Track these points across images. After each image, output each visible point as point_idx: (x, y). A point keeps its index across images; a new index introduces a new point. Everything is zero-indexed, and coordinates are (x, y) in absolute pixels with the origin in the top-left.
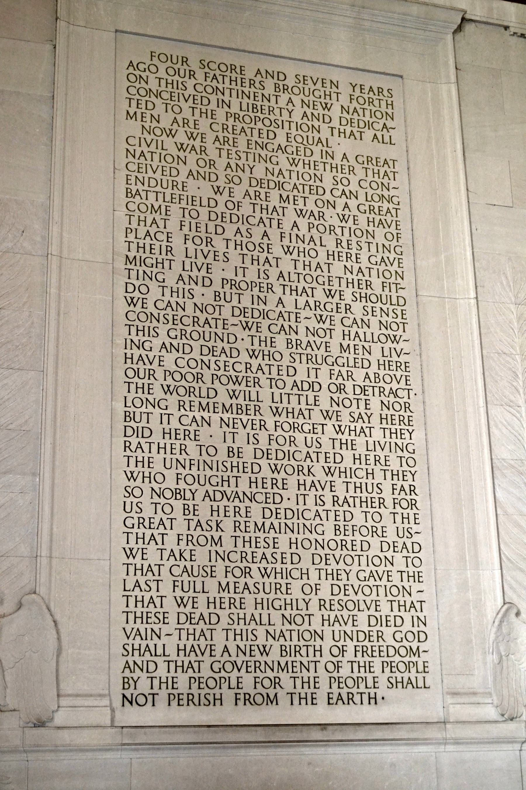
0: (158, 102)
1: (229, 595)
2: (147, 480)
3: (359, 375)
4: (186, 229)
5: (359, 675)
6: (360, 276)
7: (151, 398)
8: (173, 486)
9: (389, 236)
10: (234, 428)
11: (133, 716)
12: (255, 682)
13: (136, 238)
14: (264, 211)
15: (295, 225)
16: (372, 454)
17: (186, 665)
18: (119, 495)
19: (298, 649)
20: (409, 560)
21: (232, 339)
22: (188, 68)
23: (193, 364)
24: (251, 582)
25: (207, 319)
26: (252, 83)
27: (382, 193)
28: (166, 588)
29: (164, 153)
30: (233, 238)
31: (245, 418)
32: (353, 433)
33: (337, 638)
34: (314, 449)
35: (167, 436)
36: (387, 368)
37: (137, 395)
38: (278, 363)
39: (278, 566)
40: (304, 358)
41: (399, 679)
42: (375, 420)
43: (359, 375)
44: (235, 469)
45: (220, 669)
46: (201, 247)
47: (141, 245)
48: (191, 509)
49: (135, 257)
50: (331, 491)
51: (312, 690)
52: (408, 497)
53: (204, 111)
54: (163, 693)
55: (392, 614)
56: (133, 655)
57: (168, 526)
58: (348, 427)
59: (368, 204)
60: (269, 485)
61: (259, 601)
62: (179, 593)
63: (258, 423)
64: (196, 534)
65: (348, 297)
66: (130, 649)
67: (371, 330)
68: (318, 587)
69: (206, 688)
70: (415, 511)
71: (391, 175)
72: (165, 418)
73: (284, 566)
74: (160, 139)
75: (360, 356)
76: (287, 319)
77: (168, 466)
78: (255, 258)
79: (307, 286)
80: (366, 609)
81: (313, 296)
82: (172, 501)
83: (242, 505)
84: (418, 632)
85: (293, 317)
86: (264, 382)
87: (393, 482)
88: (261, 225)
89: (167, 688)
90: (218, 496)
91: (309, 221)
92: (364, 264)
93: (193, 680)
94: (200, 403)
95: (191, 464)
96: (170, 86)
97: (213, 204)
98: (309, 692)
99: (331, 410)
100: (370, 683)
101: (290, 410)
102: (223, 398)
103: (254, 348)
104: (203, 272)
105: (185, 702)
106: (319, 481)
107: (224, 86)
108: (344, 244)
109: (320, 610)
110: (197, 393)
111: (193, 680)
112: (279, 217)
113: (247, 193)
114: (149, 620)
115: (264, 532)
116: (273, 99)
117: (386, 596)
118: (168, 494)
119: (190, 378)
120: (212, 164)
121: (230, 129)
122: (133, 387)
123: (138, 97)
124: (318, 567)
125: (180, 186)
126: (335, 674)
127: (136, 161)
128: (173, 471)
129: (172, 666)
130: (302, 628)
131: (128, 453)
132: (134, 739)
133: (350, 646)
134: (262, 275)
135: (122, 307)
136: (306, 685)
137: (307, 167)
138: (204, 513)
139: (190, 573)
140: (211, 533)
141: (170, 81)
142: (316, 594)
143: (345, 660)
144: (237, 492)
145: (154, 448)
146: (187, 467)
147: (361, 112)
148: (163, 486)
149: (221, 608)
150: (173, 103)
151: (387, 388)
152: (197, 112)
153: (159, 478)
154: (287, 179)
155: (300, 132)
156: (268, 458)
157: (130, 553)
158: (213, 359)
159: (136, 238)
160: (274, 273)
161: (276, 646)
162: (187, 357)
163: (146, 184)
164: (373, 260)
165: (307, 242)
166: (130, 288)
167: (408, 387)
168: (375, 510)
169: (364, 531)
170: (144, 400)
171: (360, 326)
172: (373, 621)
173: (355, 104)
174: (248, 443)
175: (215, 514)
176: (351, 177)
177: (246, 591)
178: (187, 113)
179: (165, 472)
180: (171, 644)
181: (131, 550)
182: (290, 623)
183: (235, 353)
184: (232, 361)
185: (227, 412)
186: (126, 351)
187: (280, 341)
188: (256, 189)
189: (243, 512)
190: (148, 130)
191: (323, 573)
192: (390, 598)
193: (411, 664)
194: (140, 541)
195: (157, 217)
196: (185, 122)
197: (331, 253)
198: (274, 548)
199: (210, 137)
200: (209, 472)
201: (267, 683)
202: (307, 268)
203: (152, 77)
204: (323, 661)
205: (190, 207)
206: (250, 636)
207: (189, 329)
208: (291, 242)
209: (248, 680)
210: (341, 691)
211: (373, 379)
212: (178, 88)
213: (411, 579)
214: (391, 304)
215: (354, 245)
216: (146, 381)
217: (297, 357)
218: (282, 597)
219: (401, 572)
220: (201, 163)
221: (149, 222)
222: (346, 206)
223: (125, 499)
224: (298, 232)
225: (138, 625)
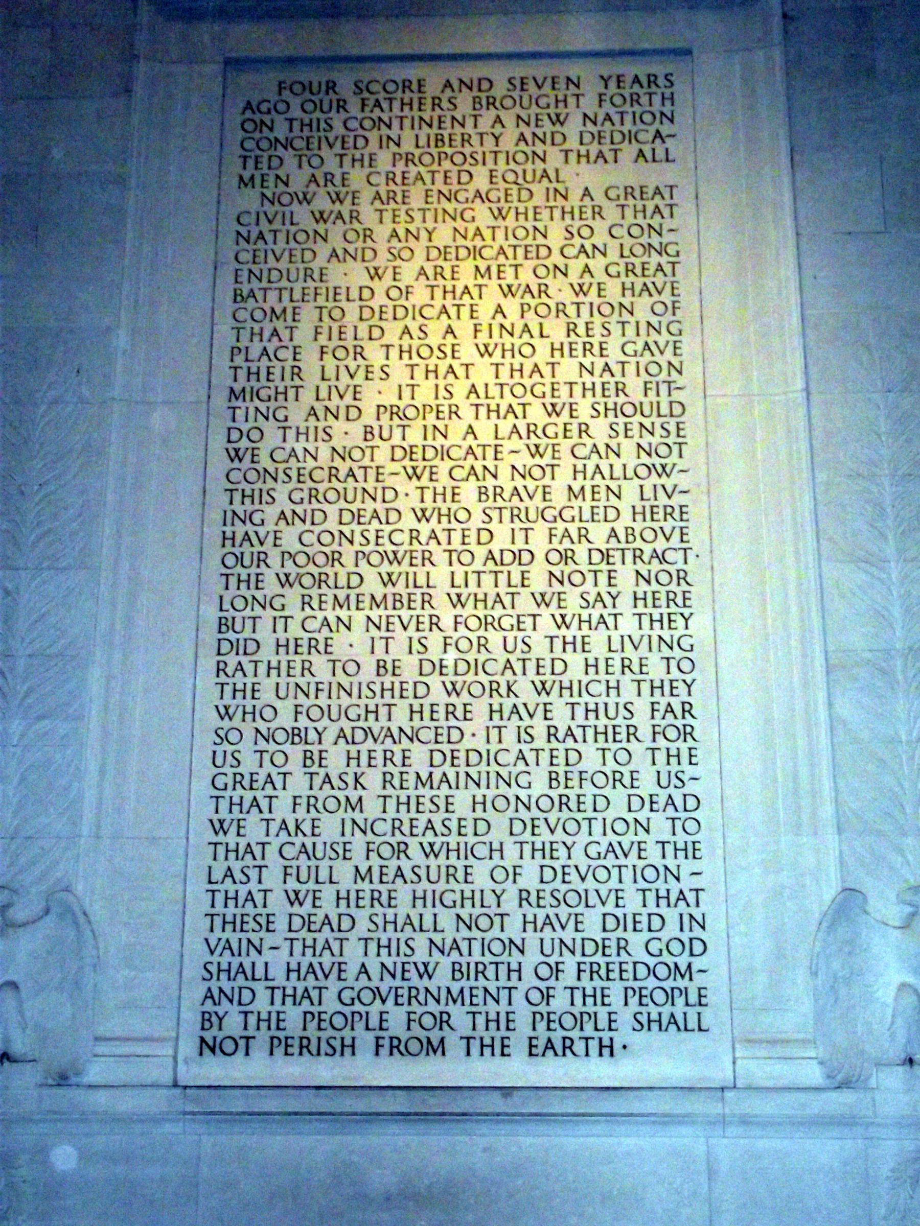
1: (372, 887)
2: (249, 717)
3: (599, 534)
4: (323, 339)
5: (584, 1009)
6: (607, 377)
7: (259, 595)
8: (289, 724)
9: (659, 308)
10: (388, 630)
11: (214, 1070)
12: (409, 1020)
13: (247, 360)
14: (449, 296)
15: (499, 310)
16: (617, 657)
17: (300, 992)
18: (205, 742)
19: (481, 967)
20: (678, 824)
21: (390, 495)
22: (334, 97)
23: (326, 538)
24: (406, 866)
25: (351, 469)
26: (436, 103)
27: (649, 241)
28: (272, 878)
30: (397, 342)
31: (405, 614)
32: (585, 626)
33: (547, 951)
35: (282, 650)
37: (239, 593)
38: (463, 526)
39: (453, 840)
40: (506, 514)
41: (654, 1016)
42: (625, 604)
43: (599, 534)
44: (387, 694)
45: (353, 999)
46: (345, 363)
48: (316, 757)
49: (243, 390)
50: (546, 718)
51: (503, 1032)
52: (679, 723)
55: (645, 911)
56: (218, 979)
57: (279, 785)
59: (622, 262)
60: (442, 715)
62: (292, 884)
63: (426, 620)
64: (321, 795)
65: (584, 411)
66: (213, 969)
67: (623, 460)
68: (518, 870)
69: (330, 1028)
71: (666, 212)
73: (462, 839)
74: (287, 209)
75: (602, 504)
77: (282, 694)
78: (431, 368)
79: (514, 402)
80: (599, 904)
81: (525, 417)
82: (287, 748)
83: (397, 749)
84: (691, 939)
85: (490, 452)
86: (440, 557)
87: (653, 700)
88: (444, 316)
89: (269, 1028)
91: (523, 301)
92: (614, 354)
93: (309, 1017)
94: (335, 596)
95: (317, 690)
96: (306, 129)
97: (366, 293)
98: (498, 1035)
99: (549, 591)
100: (603, 1023)
101: (481, 597)
102: (373, 586)
103: (423, 506)
104: (348, 399)
105: (296, 1050)
107: (391, 114)
108: (581, 330)
109: (521, 906)
110: (331, 582)
111: (309, 1017)
112: (472, 302)
114: (245, 927)
115: (432, 788)
116: (470, 122)
117: (635, 881)
118: (280, 736)
119: (321, 560)
120: (368, 234)
121: (399, 180)
122: (233, 581)
125: (316, 276)
126: (543, 1008)
127: (251, 247)
128: (290, 703)
129: (278, 994)
130: (488, 936)
131: (223, 678)
132: (206, 1106)
133: (570, 963)
134: (442, 393)
136: (492, 1025)
138: (335, 761)
139: (311, 854)
140: (346, 793)
143: (560, 985)
145: (262, 668)
146: (312, 696)
147: (616, 118)
148: (273, 725)
149: (358, 906)
150: (308, 153)
151: (648, 549)
152: (347, 161)
154: (489, 241)
155: (512, 165)
156: (441, 674)
157: (220, 827)
158: (358, 529)
159: (247, 360)
160: (460, 388)
161: (445, 963)
162: (317, 529)
163: (265, 279)
164: (629, 349)
165: (517, 332)
166: (235, 435)
167: (684, 545)
168: (619, 745)
169: (600, 780)
170: (250, 600)
173: (607, 106)
174: (410, 652)
175: (353, 763)
176: (597, 224)
177: (399, 880)
179: (278, 704)
180: (278, 961)
181: (221, 822)
182: (470, 928)
183: (393, 516)
184: (388, 529)
185: (378, 606)
186: (225, 529)
187: (468, 491)
188: (434, 263)
189: (398, 759)
191: (527, 848)
192: (642, 884)
193: (676, 992)
194: (236, 809)
195: (279, 325)
196: (329, 178)
197: (557, 346)
198: (447, 811)
199: (367, 194)
200: (345, 701)
201: (428, 1021)
202: (517, 374)
204: (523, 986)
205: (331, 304)
206: (403, 948)
207: (322, 487)
208: (491, 337)
209: (397, 1018)
210: (551, 1034)
211: (622, 538)
212: (319, 130)
213: (681, 854)
215: (597, 330)
216: (253, 570)
217: (495, 515)
218: (457, 887)
219: (663, 843)
221: (266, 334)
222: (587, 269)
225: (228, 934)
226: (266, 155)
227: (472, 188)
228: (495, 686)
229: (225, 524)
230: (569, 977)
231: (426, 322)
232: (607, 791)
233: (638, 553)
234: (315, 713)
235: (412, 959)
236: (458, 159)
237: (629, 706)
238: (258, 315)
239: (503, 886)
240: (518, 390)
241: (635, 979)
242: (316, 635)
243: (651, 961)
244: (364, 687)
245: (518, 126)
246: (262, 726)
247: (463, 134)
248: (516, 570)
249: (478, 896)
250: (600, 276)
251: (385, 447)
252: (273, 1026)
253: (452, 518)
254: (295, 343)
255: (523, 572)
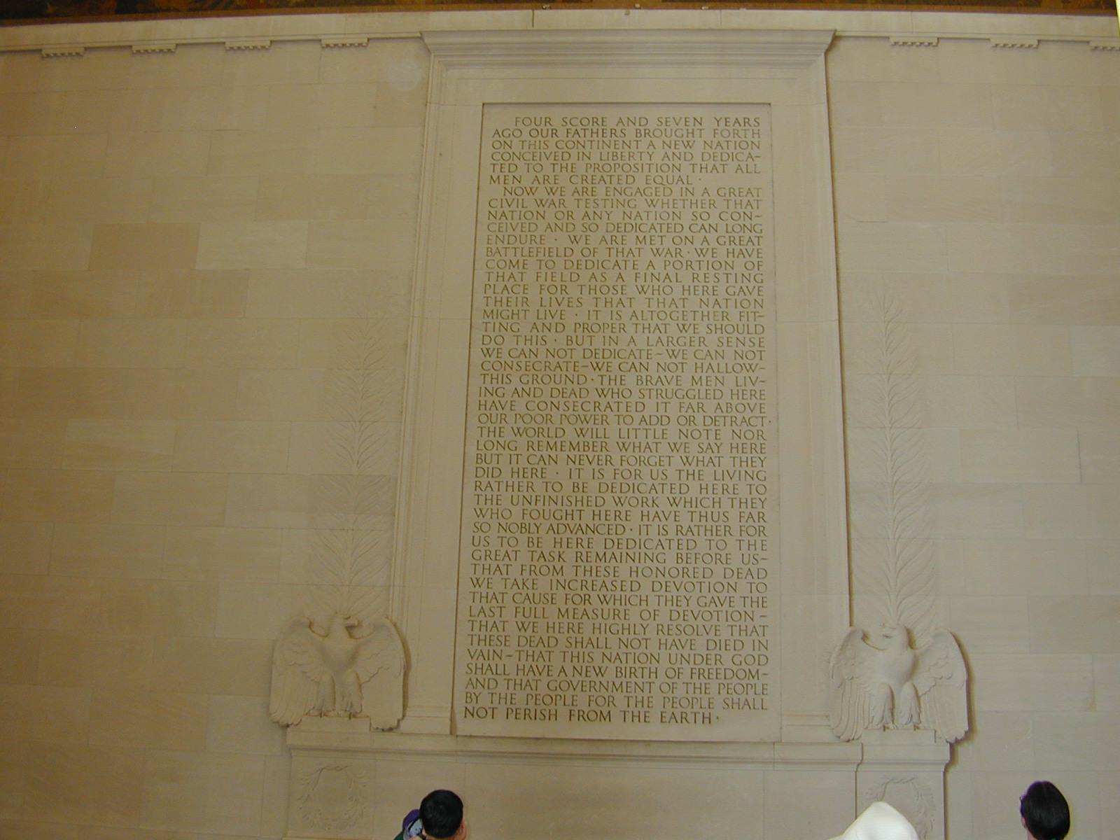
0: (520, 163)
2: (495, 516)
3: (710, 406)
4: (541, 280)
5: (693, 696)
9: (750, 266)
15: (651, 264)
16: (720, 484)
19: (633, 670)
21: (582, 380)
23: (542, 406)
27: (744, 223)
28: (508, 614)
29: (523, 210)
31: (591, 455)
33: (673, 660)
34: (659, 480)
36: (740, 397)
39: (618, 593)
40: (654, 393)
41: (736, 700)
43: (710, 406)
44: (579, 504)
46: (555, 296)
47: (499, 299)
51: (646, 708)
52: (756, 525)
53: (564, 165)
54: (502, 709)
55: (732, 639)
58: (695, 458)
61: (597, 626)
65: (702, 330)
69: (542, 704)
70: (762, 537)
72: (514, 458)
73: (623, 593)
74: (520, 198)
75: (712, 389)
76: (638, 357)
79: (660, 322)
82: (518, 535)
83: (585, 537)
84: (759, 656)
85: (644, 354)
87: (741, 510)
88: (617, 268)
89: (506, 703)
90: (562, 529)
91: (665, 259)
93: (530, 697)
95: (536, 500)
97: (569, 252)
100: (705, 704)
102: (571, 436)
103: (603, 387)
104: (557, 319)
106: (663, 512)
111: (530, 697)
113: (604, 239)
116: (634, 144)
119: (539, 419)
120: (570, 215)
121: (589, 180)
122: (485, 431)
123: (502, 162)
124: (658, 594)
125: (538, 240)
126: (670, 695)
127: (497, 221)
129: (512, 683)
133: (686, 669)
134: (615, 316)
135: (478, 357)
136: (639, 705)
137: (665, 206)
138: (547, 546)
139: (531, 600)
140: (554, 563)
141: (533, 142)
142: (654, 619)
144: (580, 525)
145: (503, 486)
146: (533, 503)
147: (725, 145)
148: (509, 521)
150: (533, 162)
152: (558, 168)
153: (506, 514)
157: (476, 583)
159: (494, 293)
161: (612, 667)
163: (506, 242)
164: (731, 291)
165: (662, 280)
166: (487, 340)
167: (762, 415)
168: (719, 538)
169: (707, 559)
170: (496, 443)
171: (714, 357)
172: (712, 645)
178: (548, 170)
179: (512, 508)
183: (584, 393)
184: (581, 401)
189: (585, 544)
190: (510, 191)
191: (663, 600)
192: (732, 623)
194: (486, 572)
195: (515, 271)
200: (553, 507)
201: (600, 701)
203: (515, 140)
205: (547, 258)
211: (724, 410)
212: (540, 148)
213: (755, 605)
214: (748, 333)
216: (498, 425)
217: (646, 393)
218: (620, 622)
220: (560, 215)
221: (506, 279)
223: (474, 534)
224: (654, 272)
226: (507, 163)
227: (635, 187)
228: (645, 500)
229: (480, 396)
230: (686, 676)
231: (605, 271)
232: (712, 566)
233: (734, 419)
234: (535, 514)
235: (592, 665)
236: (626, 168)
237: (726, 514)
238: (502, 264)
239: (648, 622)
240: (662, 315)
241: (725, 678)
242: (536, 466)
243: (735, 668)
244: (565, 499)
245: (664, 148)
246: (503, 522)
247: (629, 153)
248: (659, 429)
249: (632, 629)
250: (714, 244)
251: (580, 349)
252: (509, 702)
253: (620, 395)
254: (524, 282)
255: (663, 430)
